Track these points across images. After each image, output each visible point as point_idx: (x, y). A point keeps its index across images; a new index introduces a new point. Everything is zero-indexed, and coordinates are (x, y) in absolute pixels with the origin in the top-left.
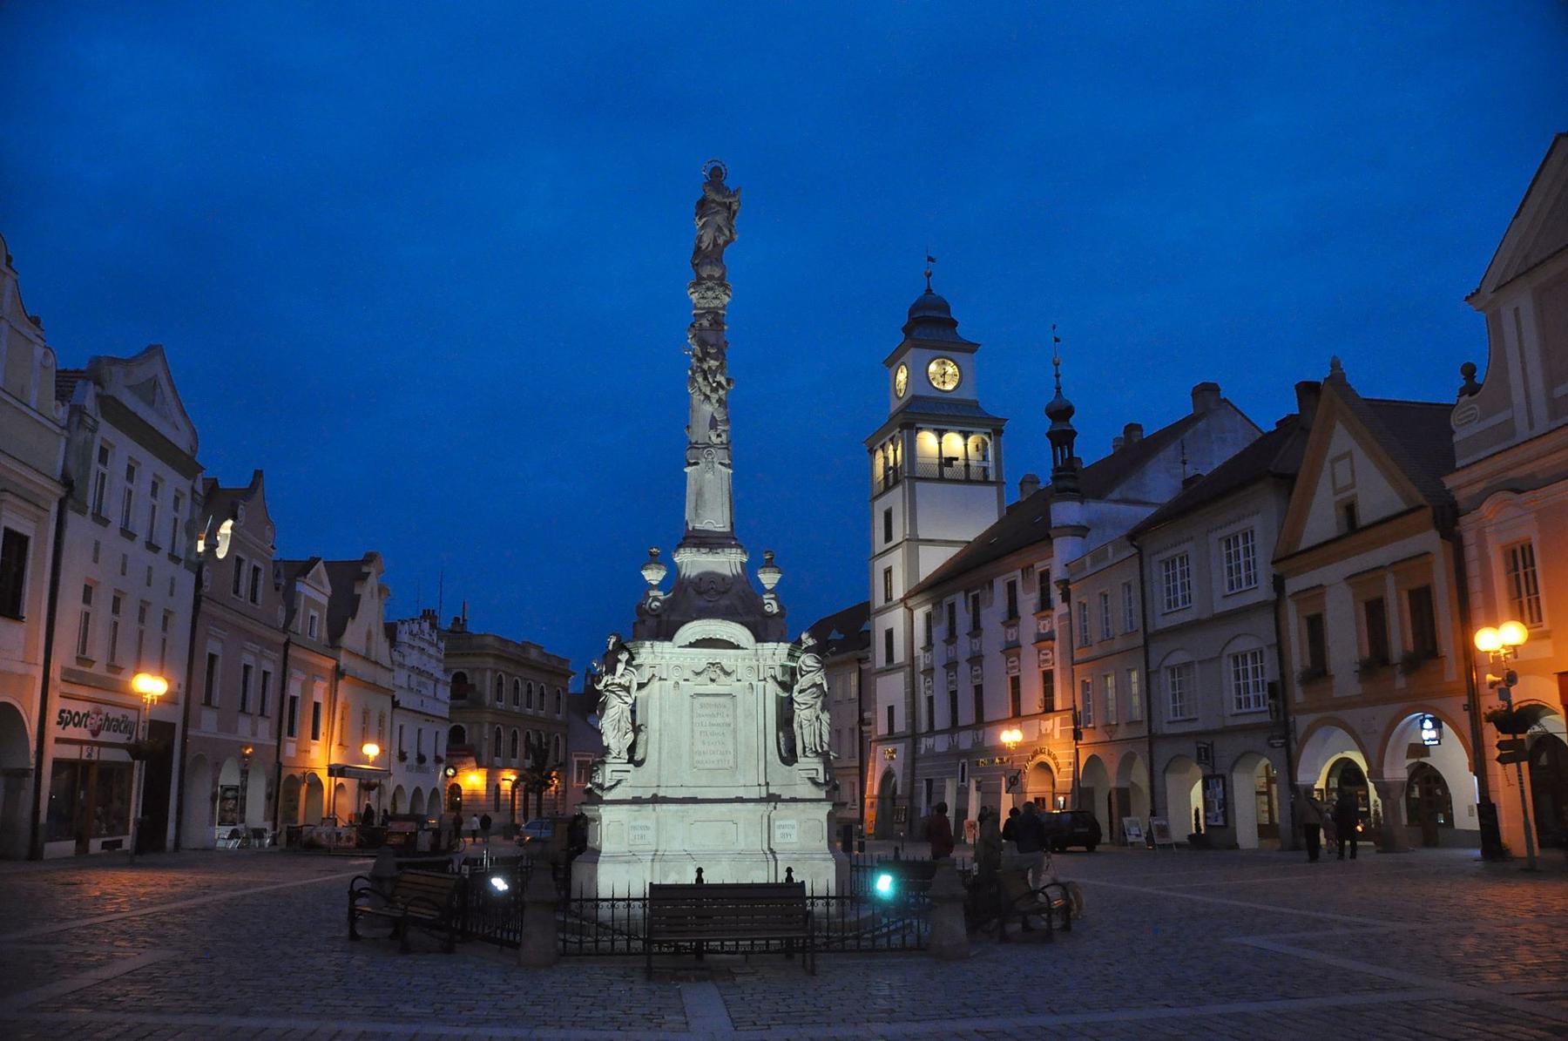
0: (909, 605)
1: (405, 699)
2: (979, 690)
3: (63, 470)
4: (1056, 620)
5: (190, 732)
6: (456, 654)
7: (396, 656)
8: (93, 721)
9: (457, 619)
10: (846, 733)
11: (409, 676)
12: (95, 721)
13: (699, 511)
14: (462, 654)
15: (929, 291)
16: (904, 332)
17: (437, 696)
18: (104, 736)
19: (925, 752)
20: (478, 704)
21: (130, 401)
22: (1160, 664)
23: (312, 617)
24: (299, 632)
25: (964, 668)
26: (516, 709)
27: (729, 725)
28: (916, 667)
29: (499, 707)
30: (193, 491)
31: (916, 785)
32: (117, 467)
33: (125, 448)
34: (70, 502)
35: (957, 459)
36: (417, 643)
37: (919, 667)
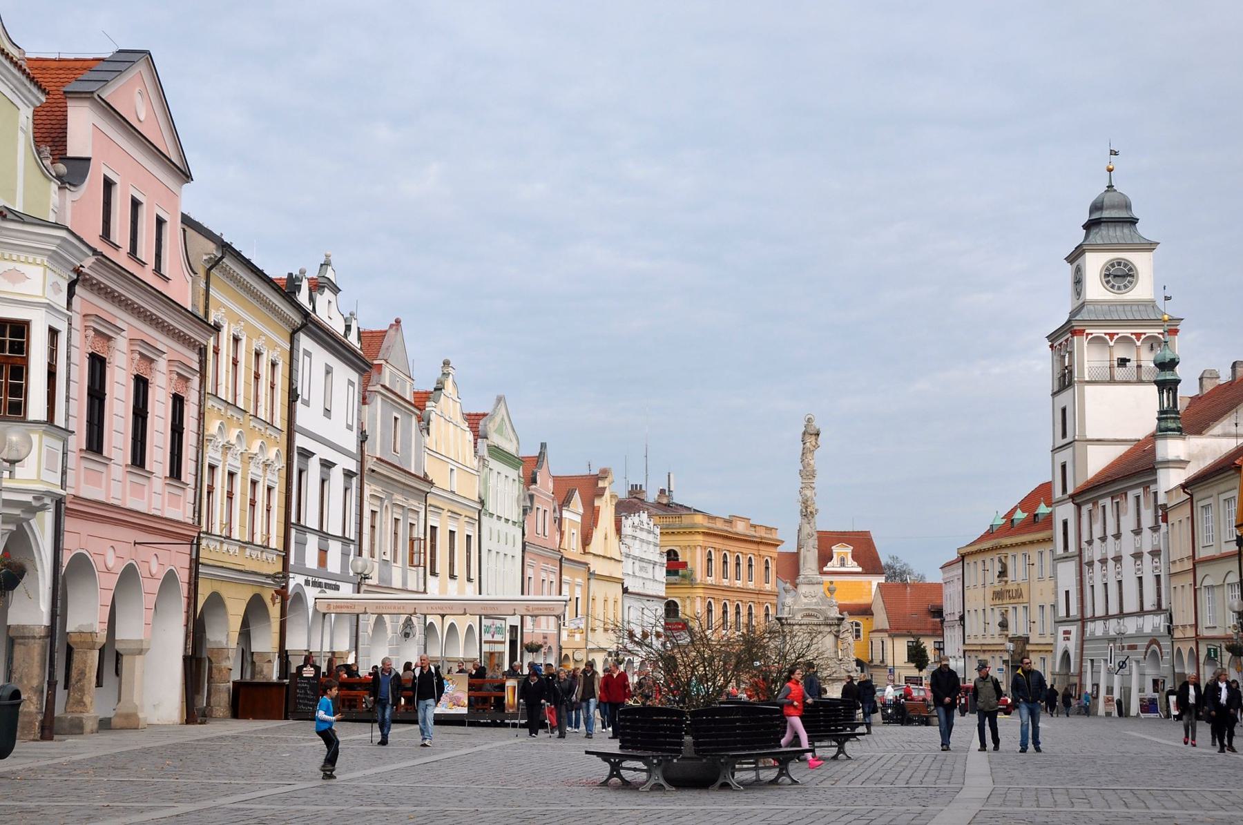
0: (1077, 501)
1: (633, 585)
2: (1120, 582)
3: (479, 494)
4: (1161, 535)
5: (524, 631)
7: (623, 547)
9: (662, 491)
10: (1048, 609)
12: (492, 630)
14: (673, 533)
15: (1110, 187)
16: (1084, 229)
18: (495, 639)
19: (1090, 635)
20: (689, 580)
22: (1201, 585)
23: (573, 534)
25: (1111, 563)
26: (726, 582)
28: (1083, 560)
29: (710, 582)
30: (519, 476)
31: (1084, 664)
35: (1129, 360)
36: (639, 534)
37: (1085, 555)
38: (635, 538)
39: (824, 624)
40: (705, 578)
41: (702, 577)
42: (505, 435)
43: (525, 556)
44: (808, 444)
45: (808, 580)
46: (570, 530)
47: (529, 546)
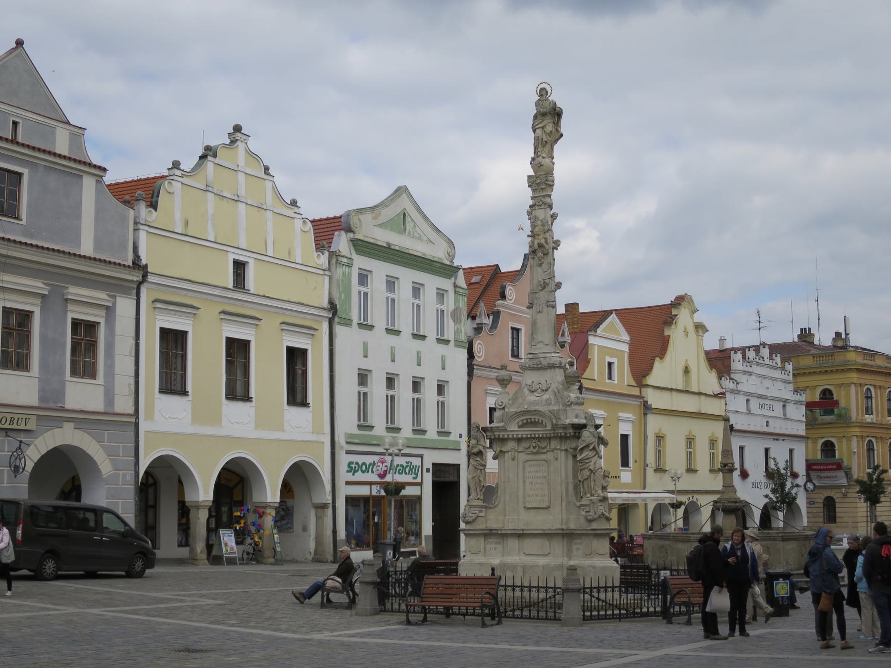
1: (738, 422)
6: (815, 372)
7: (728, 385)
8: (378, 468)
9: (838, 334)
11: (748, 401)
12: (382, 468)
13: (534, 336)
14: (826, 371)
17: (788, 416)
20: (844, 420)
21: (382, 237)
24: (596, 379)
27: (545, 477)
29: (869, 420)
30: (456, 286)
32: (377, 286)
33: (380, 270)
34: (336, 319)
38: (750, 373)
39: (555, 437)
40: (863, 416)
41: (858, 415)
42: (409, 233)
43: (473, 383)
44: (539, 131)
45: (535, 361)
46: (601, 360)
47: (477, 369)
